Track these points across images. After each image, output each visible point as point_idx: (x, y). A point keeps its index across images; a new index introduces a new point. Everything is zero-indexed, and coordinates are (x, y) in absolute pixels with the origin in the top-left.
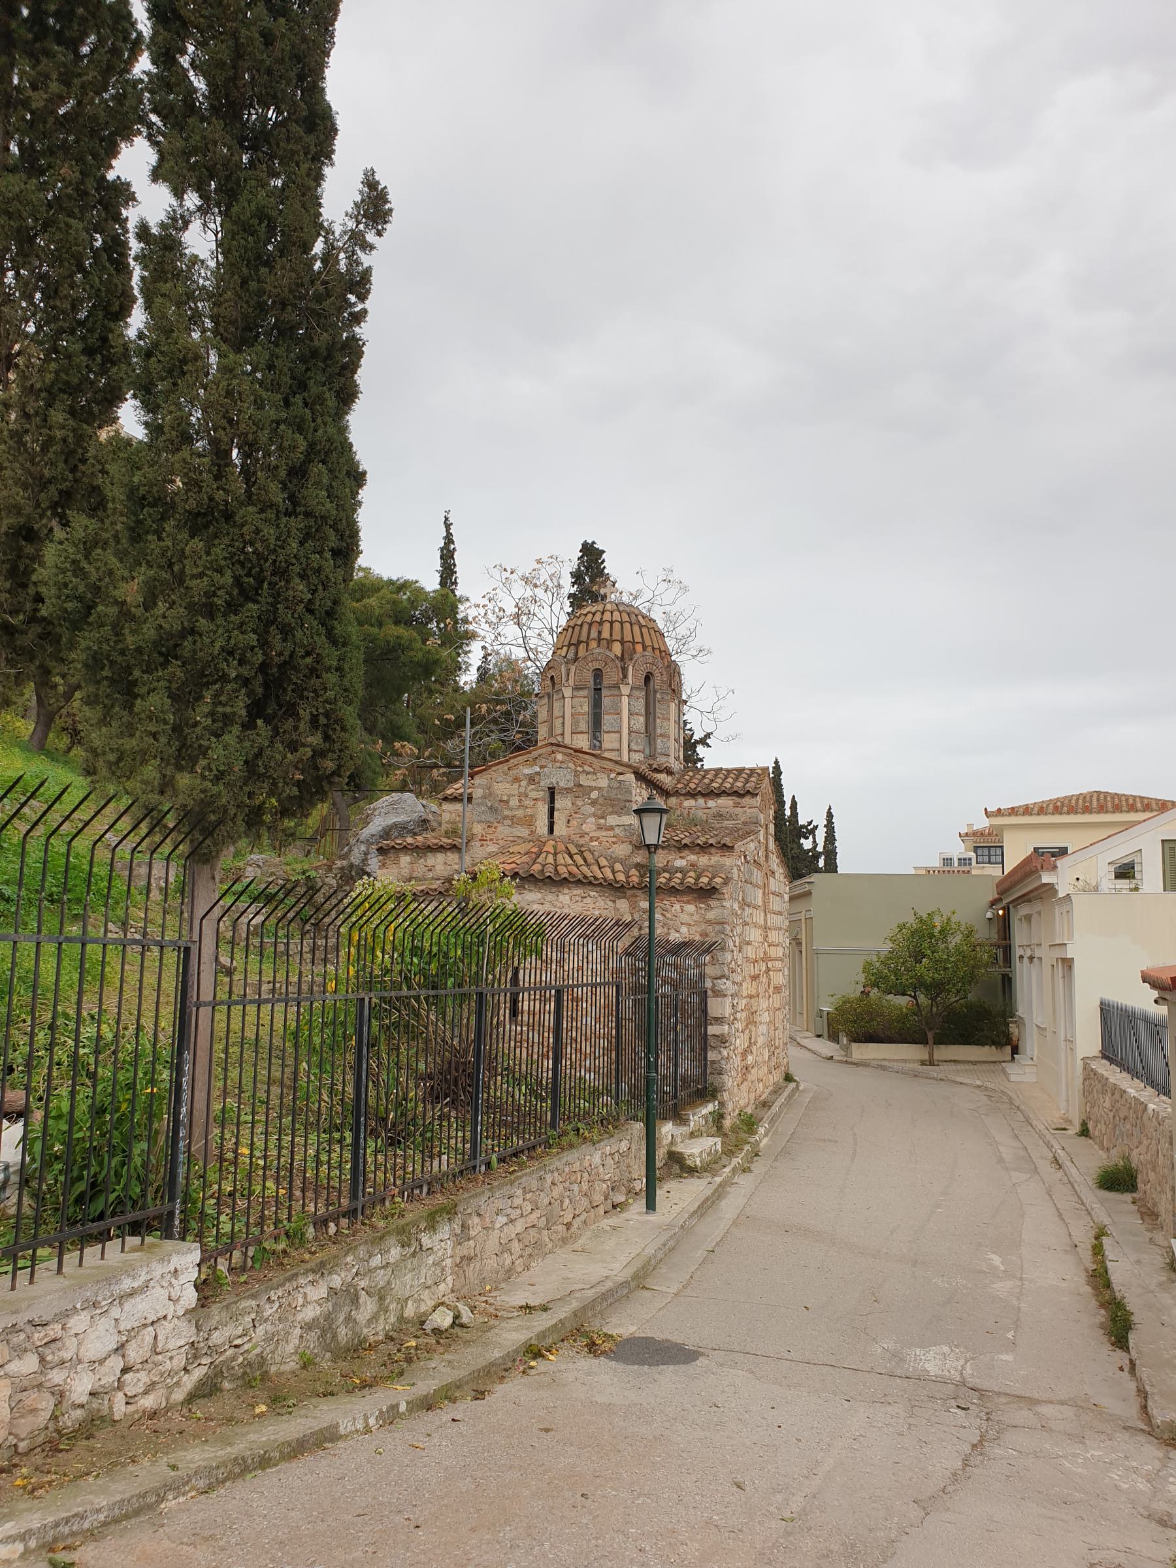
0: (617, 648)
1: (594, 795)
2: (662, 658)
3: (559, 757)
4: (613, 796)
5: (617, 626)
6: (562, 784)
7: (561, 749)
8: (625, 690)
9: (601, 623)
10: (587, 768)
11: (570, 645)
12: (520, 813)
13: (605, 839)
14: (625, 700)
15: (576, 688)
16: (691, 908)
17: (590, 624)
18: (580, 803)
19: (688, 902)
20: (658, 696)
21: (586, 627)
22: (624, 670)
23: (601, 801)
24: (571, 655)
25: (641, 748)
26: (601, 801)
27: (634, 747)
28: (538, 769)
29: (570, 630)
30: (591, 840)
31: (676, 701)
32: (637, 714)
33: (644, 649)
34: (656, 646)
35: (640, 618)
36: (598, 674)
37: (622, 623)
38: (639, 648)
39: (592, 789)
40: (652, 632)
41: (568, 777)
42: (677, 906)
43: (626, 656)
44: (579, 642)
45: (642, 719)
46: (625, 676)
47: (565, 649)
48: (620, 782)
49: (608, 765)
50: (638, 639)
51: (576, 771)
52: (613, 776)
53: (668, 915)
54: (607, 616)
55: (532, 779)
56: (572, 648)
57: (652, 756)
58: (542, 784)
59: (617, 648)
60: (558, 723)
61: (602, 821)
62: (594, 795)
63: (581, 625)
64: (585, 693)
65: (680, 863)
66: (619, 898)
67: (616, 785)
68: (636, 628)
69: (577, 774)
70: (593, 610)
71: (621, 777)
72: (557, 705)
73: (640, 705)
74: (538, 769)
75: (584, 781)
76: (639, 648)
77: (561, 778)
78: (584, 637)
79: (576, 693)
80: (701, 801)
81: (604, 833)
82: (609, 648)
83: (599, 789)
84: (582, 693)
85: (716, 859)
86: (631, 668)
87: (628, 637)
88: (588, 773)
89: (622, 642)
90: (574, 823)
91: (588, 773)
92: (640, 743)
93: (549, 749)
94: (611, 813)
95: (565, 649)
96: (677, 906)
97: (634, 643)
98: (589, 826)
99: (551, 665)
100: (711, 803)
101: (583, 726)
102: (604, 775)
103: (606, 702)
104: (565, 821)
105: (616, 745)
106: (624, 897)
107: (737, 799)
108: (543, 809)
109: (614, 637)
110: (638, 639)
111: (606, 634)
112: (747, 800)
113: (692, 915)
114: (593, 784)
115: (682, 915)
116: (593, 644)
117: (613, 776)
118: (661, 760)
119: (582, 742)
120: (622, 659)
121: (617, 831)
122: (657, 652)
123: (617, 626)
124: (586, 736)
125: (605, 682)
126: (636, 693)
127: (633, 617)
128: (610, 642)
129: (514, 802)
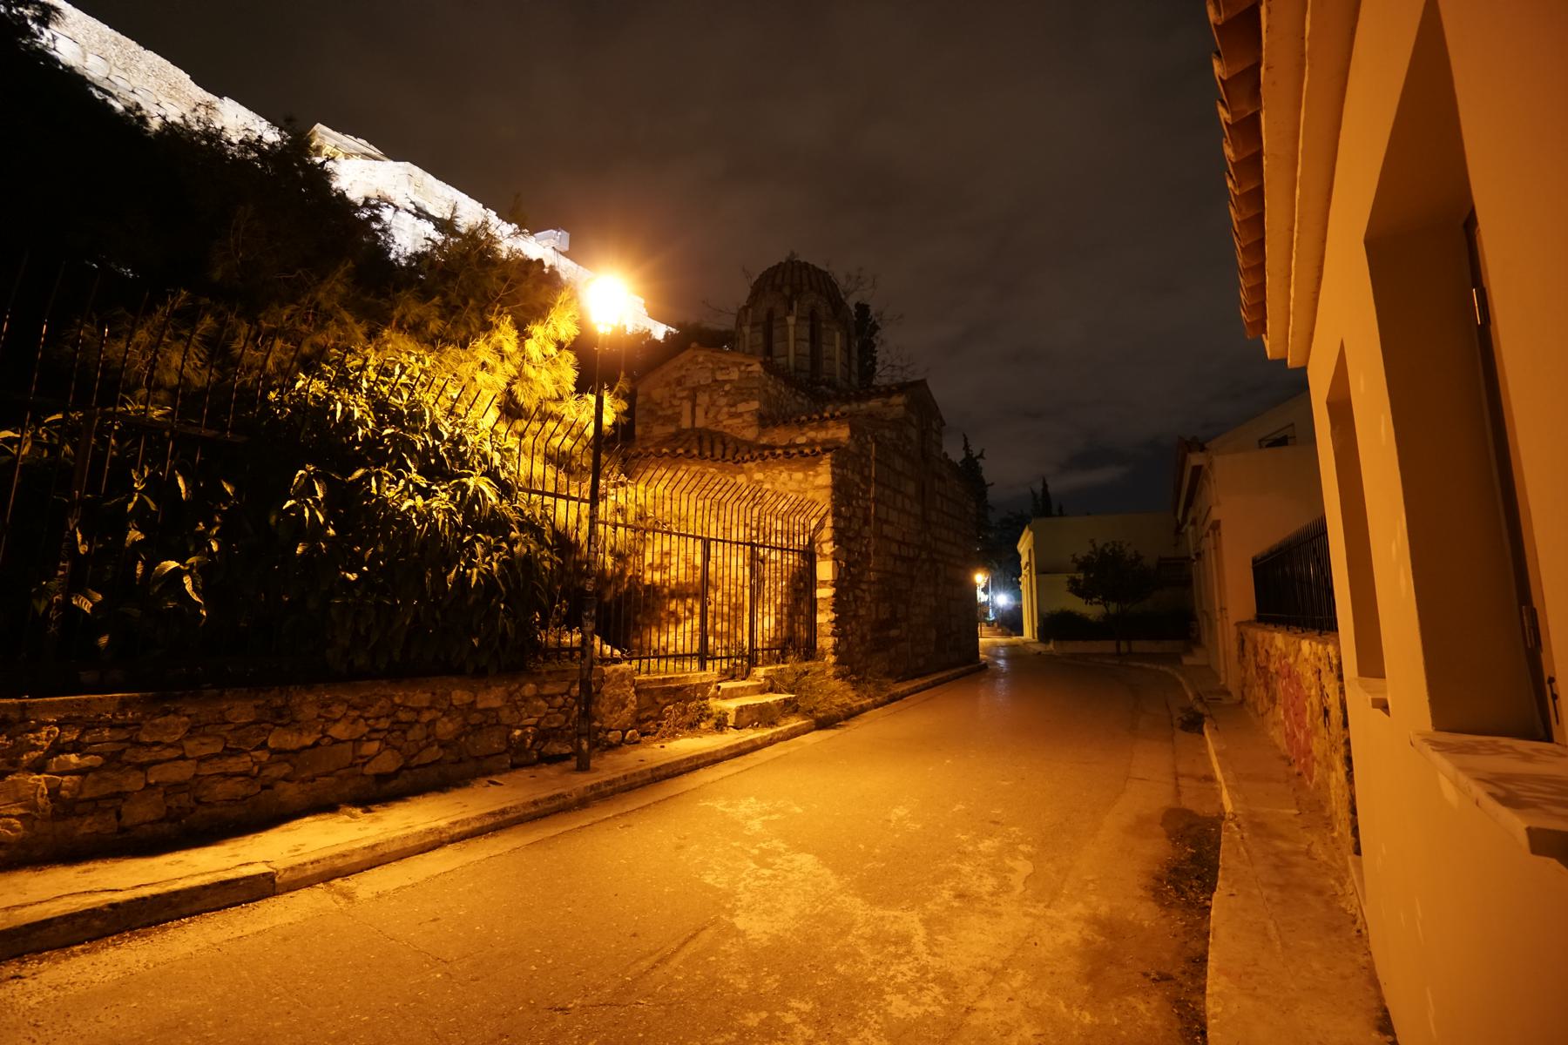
1: (727, 387)
8: (791, 320)
12: (669, 412)
16: (799, 476)
38: (806, 288)
39: (726, 382)
45: (807, 345)
46: (791, 308)
55: (679, 382)
59: (787, 291)
62: (727, 387)
65: (801, 440)
69: (713, 371)
73: (806, 333)
75: (720, 376)
90: (711, 415)
96: (785, 474)
103: (776, 333)
108: (687, 405)
129: (665, 405)
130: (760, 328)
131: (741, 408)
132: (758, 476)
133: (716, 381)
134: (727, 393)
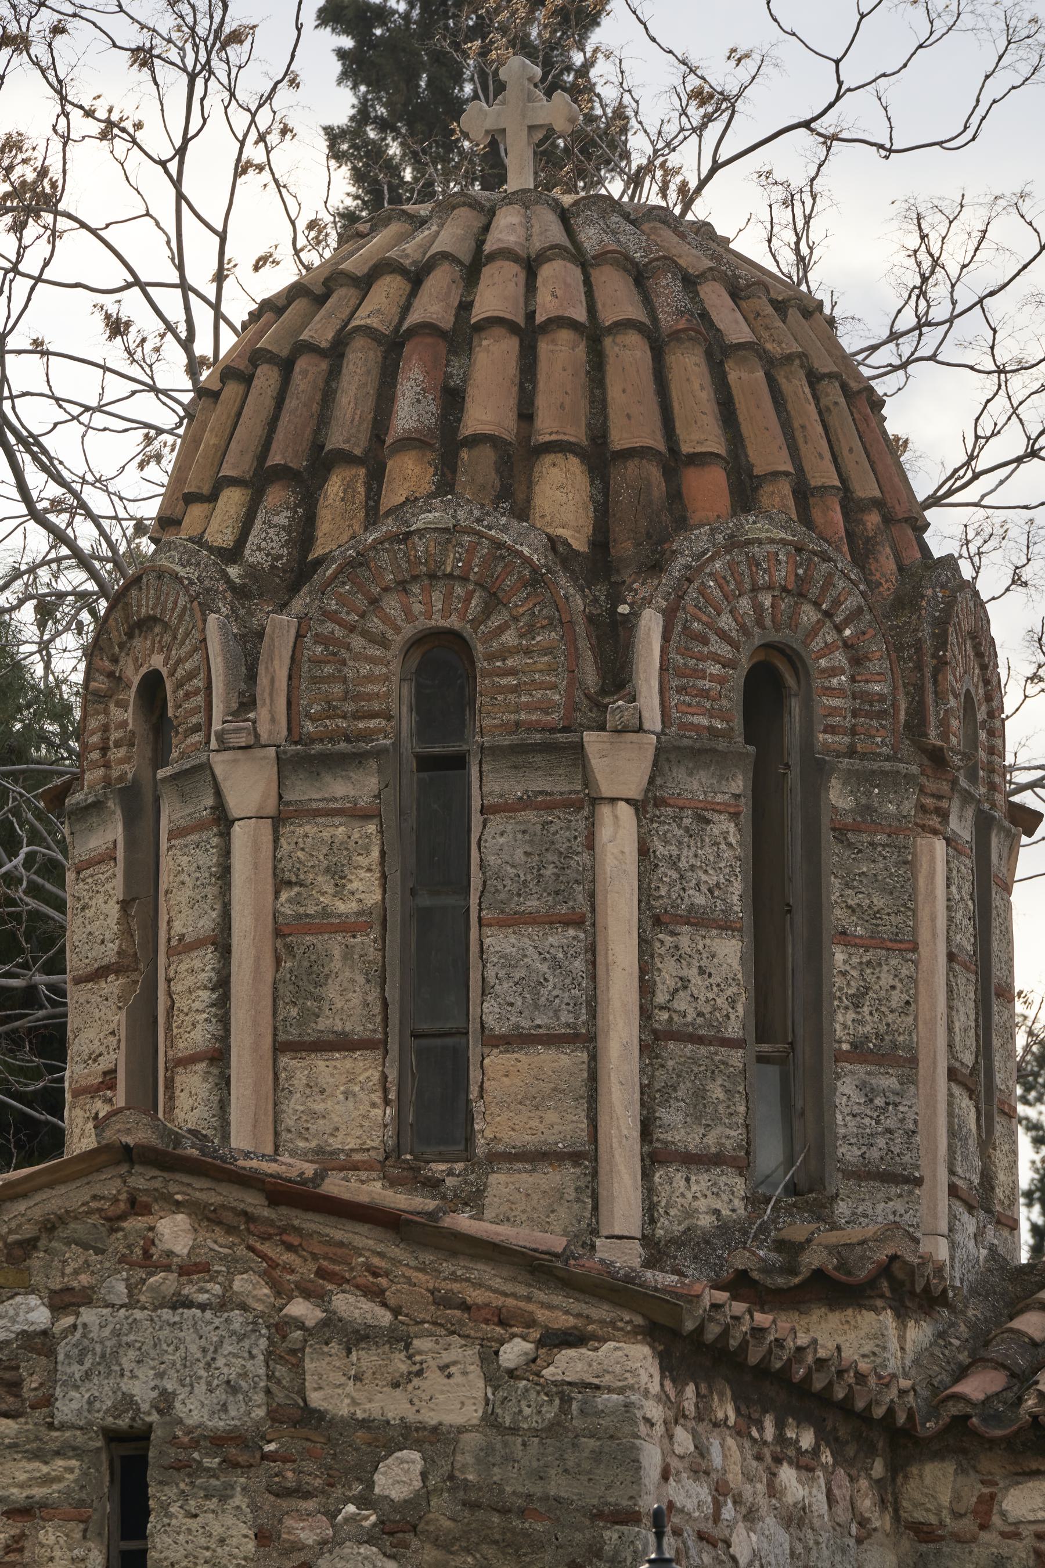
0: (562, 498)
1: (398, 1477)
2: (861, 552)
3: (175, 1233)
4: (514, 1483)
5: (561, 358)
6: (195, 1409)
7: (180, 1187)
8: (619, 767)
9: (461, 336)
10: (351, 1306)
11: (260, 480)
14: (618, 834)
15: (301, 760)
17: (393, 346)
20: (839, 797)
21: (359, 366)
22: (614, 640)
23: (442, 1514)
24: (267, 543)
25: (725, 1136)
26: (442, 1514)
27: (679, 1130)
28: (39, 1315)
29: (266, 378)
31: (961, 826)
32: (699, 920)
33: (745, 489)
34: (822, 473)
35: (715, 298)
36: (443, 666)
37: (594, 335)
39: (387, 1438)
40: (796, 387)
41: (227, 1367)
43: (624, 547)
44: (322, 462)
45: (729, 952)
46: (617, 677)
47: (232, 500)
48: (563, 1392)
49: (488, 1286)
50: (701, 433)
51: (282, 1327)
52: (514, 1352)
54: (497, 294)
56: (276, 496)
57: (808, 1192)
58: (69, 1406)
59: (562, 498)
60: (188, 979)
62: (398, 1477)
63: (335, 353)
64: (361, 786)
67: (533, 1410)
68: (689, 367)
69: (285, 1345)
70: (411, 250)
71: (569, 1364)
72: (182, 866)
73: (716, 864)
74: (39, 1315)
75: (334, 1388)
76: (707, 490)
77: (194, 1371)
78: (346, 431)
79: (303, 791)
82: (513, 495)
84: (339, 788)
86: (651, 626)
87: (633, 426)
89: (599, 457)
92: (722, 1111)
93: (109, 1185)
95: (232, 500)
97: (675, 461)
99: (143, 604)
101: (349, 1000)
102: (462, 1354)
105: (561, 1126)
109: (548, 426)
110: (701, 433)
111: (487, 412)
114: (393, 1406)
116: (409, 475)
117: (514, 1352)
118: (861, 1217)
119: (348, 1107)
120: (598, 563)
122: (832, 516)
123: (561, 358)
124: (366, 1069)
125: (493, 716)
126: (693, 784)
127: (668, 291)
128: (518, 459)
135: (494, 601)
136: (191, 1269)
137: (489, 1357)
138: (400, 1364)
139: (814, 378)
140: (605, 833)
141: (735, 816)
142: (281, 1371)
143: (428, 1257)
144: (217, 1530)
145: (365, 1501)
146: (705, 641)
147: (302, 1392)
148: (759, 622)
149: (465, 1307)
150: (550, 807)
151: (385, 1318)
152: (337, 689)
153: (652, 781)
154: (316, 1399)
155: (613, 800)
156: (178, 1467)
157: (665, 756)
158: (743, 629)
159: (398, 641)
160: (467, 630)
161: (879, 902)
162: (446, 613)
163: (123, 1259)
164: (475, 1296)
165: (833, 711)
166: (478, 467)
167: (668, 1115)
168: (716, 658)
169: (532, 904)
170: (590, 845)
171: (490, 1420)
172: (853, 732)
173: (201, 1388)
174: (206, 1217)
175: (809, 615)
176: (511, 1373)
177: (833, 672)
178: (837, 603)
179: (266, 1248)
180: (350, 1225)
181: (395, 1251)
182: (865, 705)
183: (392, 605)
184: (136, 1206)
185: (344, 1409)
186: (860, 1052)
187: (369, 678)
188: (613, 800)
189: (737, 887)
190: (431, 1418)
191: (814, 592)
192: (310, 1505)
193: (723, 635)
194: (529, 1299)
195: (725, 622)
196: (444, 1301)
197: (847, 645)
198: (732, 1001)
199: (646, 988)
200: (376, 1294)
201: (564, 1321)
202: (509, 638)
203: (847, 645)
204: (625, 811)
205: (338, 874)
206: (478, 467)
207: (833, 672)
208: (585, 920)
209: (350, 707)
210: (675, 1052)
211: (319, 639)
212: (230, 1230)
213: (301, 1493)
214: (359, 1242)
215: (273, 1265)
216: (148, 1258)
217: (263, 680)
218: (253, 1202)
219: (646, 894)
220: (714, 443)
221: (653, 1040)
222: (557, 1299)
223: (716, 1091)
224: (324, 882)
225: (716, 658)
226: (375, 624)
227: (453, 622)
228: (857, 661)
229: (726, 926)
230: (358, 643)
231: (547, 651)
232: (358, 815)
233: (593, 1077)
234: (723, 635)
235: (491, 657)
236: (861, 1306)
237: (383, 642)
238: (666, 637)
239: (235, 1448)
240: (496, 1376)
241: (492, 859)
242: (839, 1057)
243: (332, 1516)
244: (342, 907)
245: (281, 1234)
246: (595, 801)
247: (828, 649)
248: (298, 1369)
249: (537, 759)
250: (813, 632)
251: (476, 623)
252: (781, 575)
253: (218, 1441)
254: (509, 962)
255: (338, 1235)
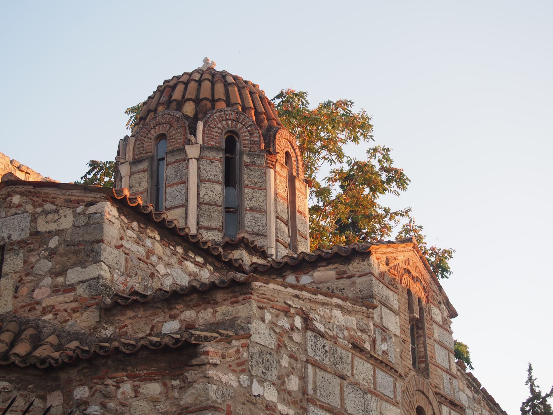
0: (189, 109)
1: (53, 243)
3: (16, 199)
6: (15, 237)
8: (192, 151)
13: (62, 307)
16: (153, 388)
18: (33, 260)
19: (150, 379)
20: (246, 159)
30: (45, 311)
33: (229, 104)
39: (51, 234)
42: (127, 387)
45: (219, 188)
48: (89, 216)
52: (80, 209)
53: (111, 405)
59: (189, 109)
61: (60, 280)
62: (53, 243)
66: (52, 390)
67: (82, 220)
69: (34, 220)
71: (91, 209)
73: (216, 170)
75: (43, 226)
79: (135, 169)
80: (291, 279)
81: (61, 298)
83: (59, 232)
85: (224, 310)
88: (50, 212)
89: (197, 101)
90: (24, 290)
91: (50, 212)
94: (74, 265)
96: (127, 387)
97: (213, 101)
98: (42, 293)
100: (305, 279)
102: (69, 212)
103: (169, 172)
104: (12, 289)
106: (57, 388)
107: (341, 267)
112: (355, 266)
113: (155, 401)
114: (53, 227)
115: (136, 403)
117: (80, 209)
121: (80, 290)
130: (145, 165)
131: (74, 275)
132: (81, 393)
133: (35, 233)
134: (52, 253)
135: (171, 126)
136: (19, 206)
137: (74, 211)
138: (56, 217)
139: (251, 93)
140: (190, 165)
141: (220, 161)
142: (33, 224)
143: (64, 191)
144: (16, 262)
145: (46, 250)
146: (214, 128)
147: (36, 228)
148: (228, 126)
149: (71, 201)
150: (179, 162)
151: (54, 207)
152: (142, 149)
153: (200, 154)
154: (39, 230)
155: (192, 158)
156: (10, 250)
157: (203, 148)
158: (224, 127)
159: (153, 138)
160: (166, 133)
161: (256, 180)
162: (162, 130)
163: (6, 207)
164: (73, 198)
165: (245, 144)
166: (174, 105)
167: (201, 220)
168: (217, 132)
169: (176, 181)
170: (187, 168)
171: (74, 225)
172: (250, 148)
173: (17, 232)
174: (22, 194)
175: (240, 125)
176: (79, 214)
177: (245, 136)
178: (246, 123)
179: (34, 198)
180: (49, 189)
181: (58, 192)
182: (253, 142)
183: (152, 131)
184: (9, 195)
185: (44, 230)
186: (251, 209)
187: (148, 146)
188: (192, 158)
189: (221, 175)
190: (61, 228)
191: (240, 121)
192: (35, 253)
193: (219, 128)
194: (84, 196)
195: (219, 125)
196: (67, 201)
197: (249, 131)
198: (219, 198)
199: (198, 194)
200: (53, 203)
201: (90, 199)
202: (174, 132)
203: (249, 131)
204: (195, 161)
205: (140, 184)
206: (174, 105)
207: (245, 136)
208: (185, 182)
209: (144, 152)
210: (204, 207)
211: (139, 140)
212: (27, 196)
213: (33, 250)
214: (51, 192)
215: (34, 201)
216: (10, 206)
217: (127, 149)
218: (31, 188)
219: (199, 176)
220: (222, 96)
221: (200, 204)
222: (90, 195)
223: (215, 215)
224: (137, 185)
225: (217, 132)
226: (149, 136)
227: (164, 132)
228: (251, 134)
229: (217, 182)
230: (146, 140)
231: (180, 132)
232: (145, 171)
233: (186, 213)
234: (219, 128)
235: (170, 137)
236: (237, 250)
237: (151, 139)
238: (204, 127)
239: (22, 243)
240: (76, 215)
241: (168, 174)
242: (246, 210)
243: (39, 255)
244: (140, 189)
245: (38, 195)
246: (188, 160)
247: (244, 132)
248: (36, 222)
249: (177, 153)
250: (241, 129)
251: (167, 131)
252: (232, 117)
253: (18, 242)
254: (170, 193)
255: (46, 191)
